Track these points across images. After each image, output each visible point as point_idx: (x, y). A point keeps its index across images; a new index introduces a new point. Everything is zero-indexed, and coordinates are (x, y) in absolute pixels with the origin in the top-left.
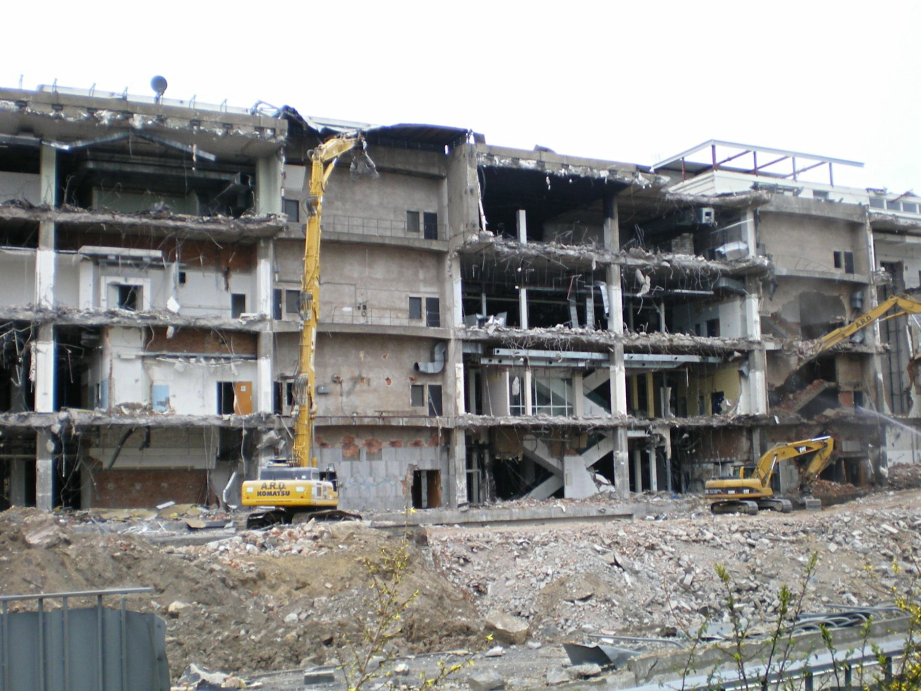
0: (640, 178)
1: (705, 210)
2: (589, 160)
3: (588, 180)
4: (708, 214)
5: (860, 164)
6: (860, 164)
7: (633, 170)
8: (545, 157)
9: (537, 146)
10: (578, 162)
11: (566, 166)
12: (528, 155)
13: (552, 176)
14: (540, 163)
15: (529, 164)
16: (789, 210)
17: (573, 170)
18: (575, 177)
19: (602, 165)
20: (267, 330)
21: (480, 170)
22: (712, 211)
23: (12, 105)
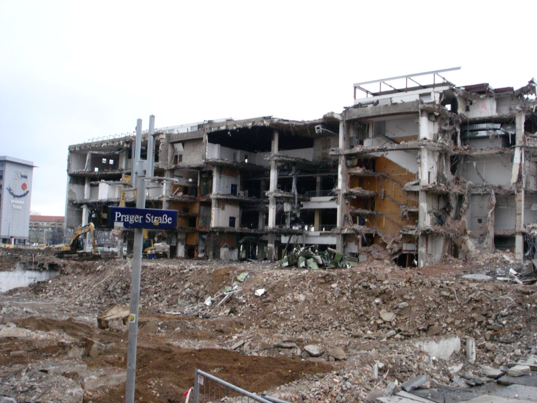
0: (265, 122)
1: (316, 127)
2: (244, 120)
3: (244, 128)
4: (318, 128)
5: (459, 68)
6: (459, 68)
7: (261, 119)
8: (229, 124)
9: (70, 148)
10: (239, 122)
11: (235, 125)
12: (223, 124)
13: (232, 131)
14: (227, 126)
15: (223, 128)
16: (365, 116)
17: (239, 126)
18: (239, 129)
19: (249, 121)
20: (164, 200)
21: (208, 134)
22: (320, 126)
23: (106, 144)
